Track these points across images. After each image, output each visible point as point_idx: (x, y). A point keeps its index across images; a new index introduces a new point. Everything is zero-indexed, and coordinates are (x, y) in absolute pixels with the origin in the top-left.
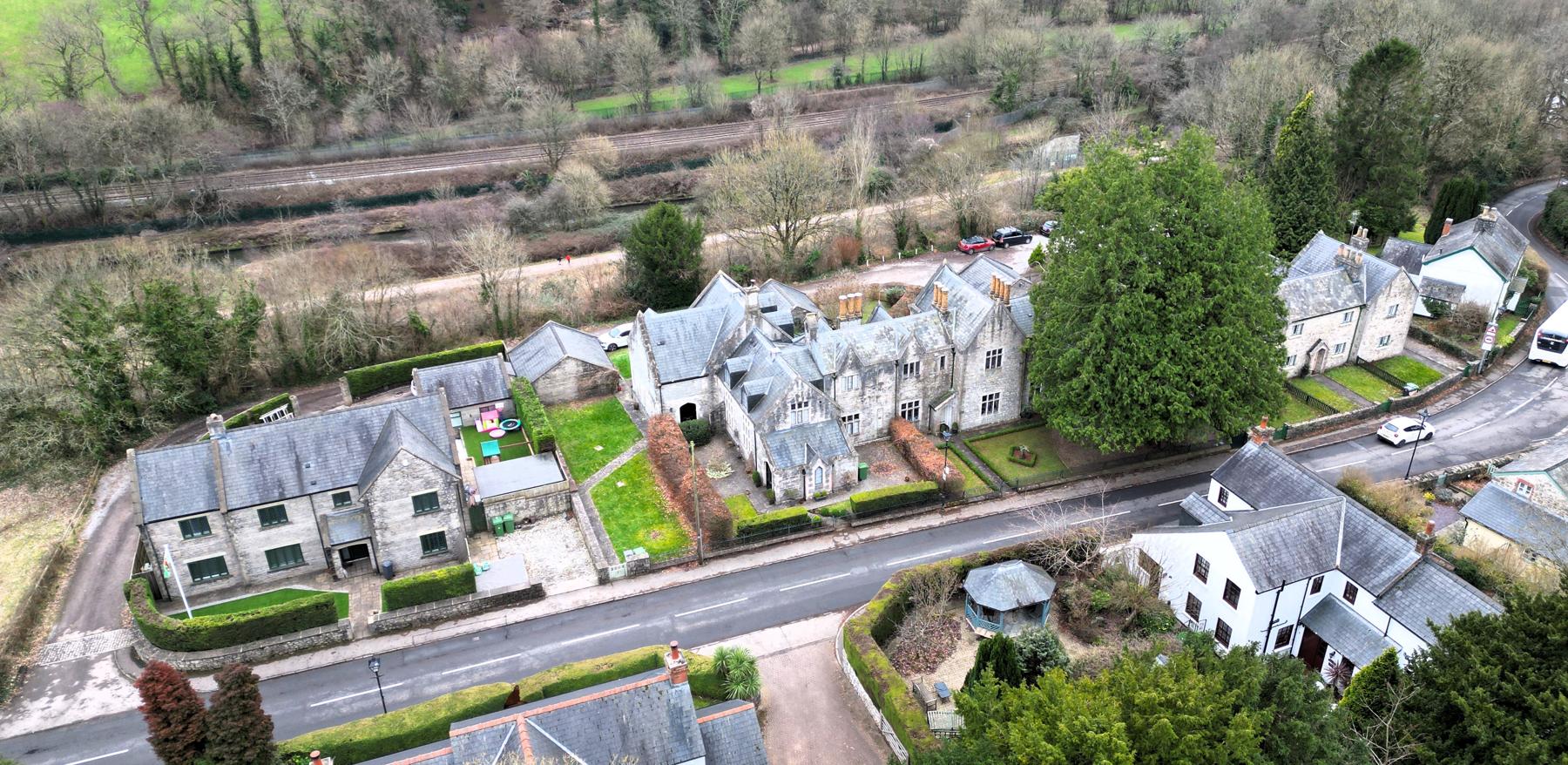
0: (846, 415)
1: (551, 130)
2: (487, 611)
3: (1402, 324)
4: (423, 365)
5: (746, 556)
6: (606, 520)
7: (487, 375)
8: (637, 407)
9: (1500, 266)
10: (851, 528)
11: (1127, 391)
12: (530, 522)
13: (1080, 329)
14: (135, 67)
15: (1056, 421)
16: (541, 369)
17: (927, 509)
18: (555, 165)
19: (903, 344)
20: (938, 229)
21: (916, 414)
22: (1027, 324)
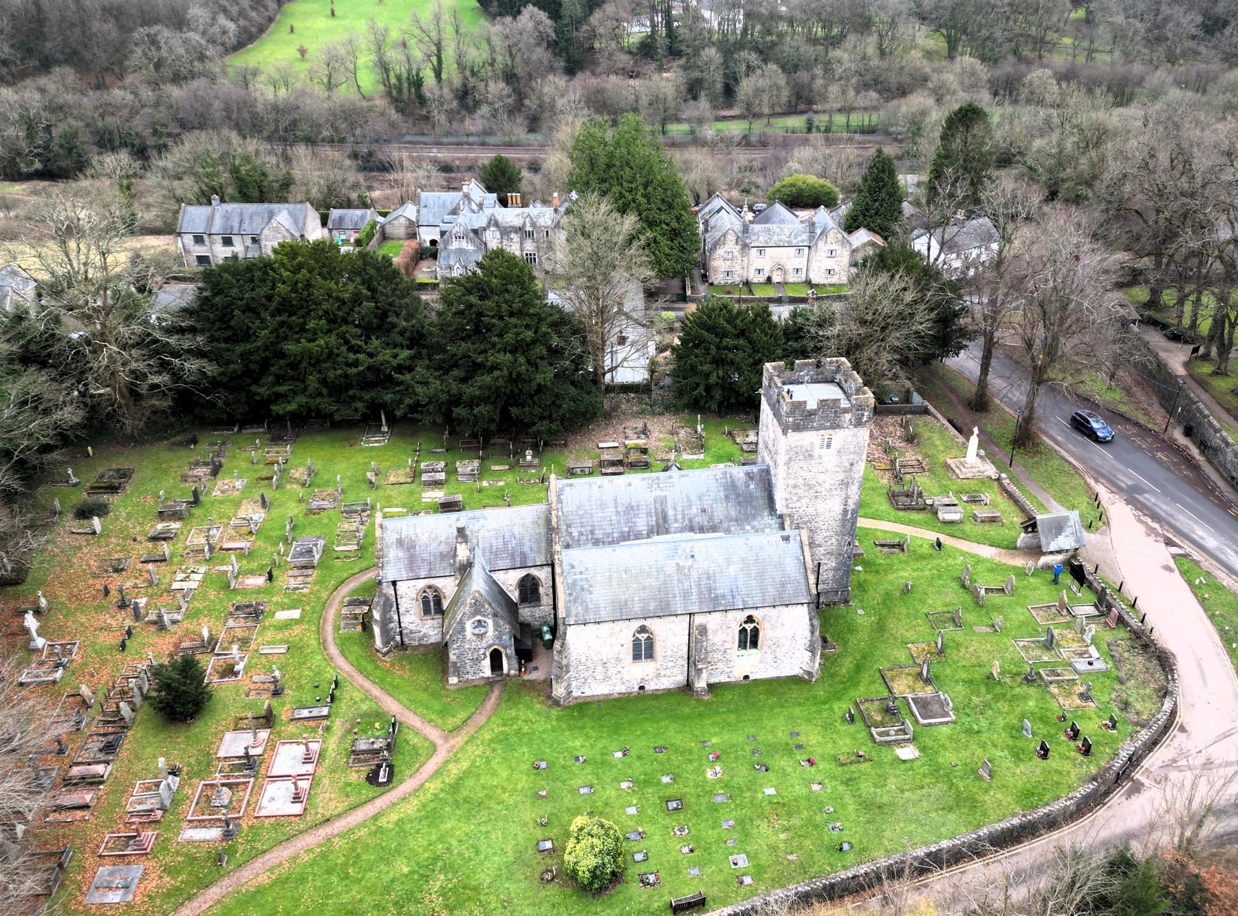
7: (363, 217)
14: (368, 80)
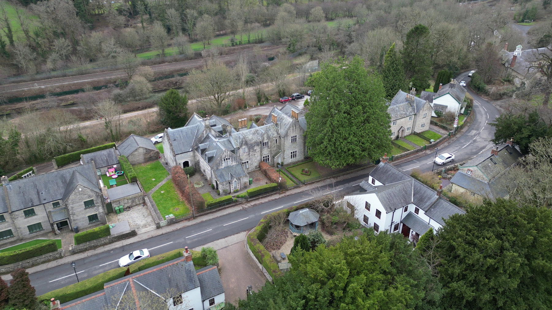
0: (244, 162)
1: (128, 65)
2: (115, 241)
3: (427, 121)
4: (84, 153)
5: (211, 214)
6: (158, 205)
7: (109, 155)
8: (167, 164)
9: (458, 99)
10: (248, 202)
11: (339, 147)
12: (129, 208)
13: (323, 127)
15: (316, 159)
16: (130, 152)
17: (274, 193)
18: (130, 78)
19: (262, 135)
20: (272, 95)
21: (268, 160)
22: (305, 127)
